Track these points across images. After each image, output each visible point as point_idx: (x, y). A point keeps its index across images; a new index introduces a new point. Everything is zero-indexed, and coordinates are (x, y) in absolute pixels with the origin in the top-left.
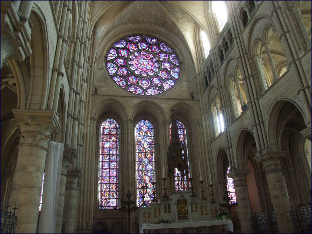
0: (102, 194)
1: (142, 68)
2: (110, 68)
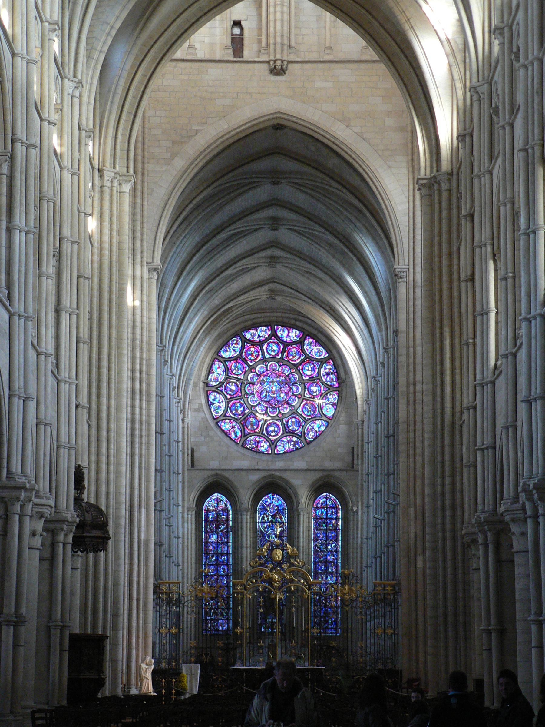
0: (207, 614)
1: (270, 400)
2: (213, 404)
